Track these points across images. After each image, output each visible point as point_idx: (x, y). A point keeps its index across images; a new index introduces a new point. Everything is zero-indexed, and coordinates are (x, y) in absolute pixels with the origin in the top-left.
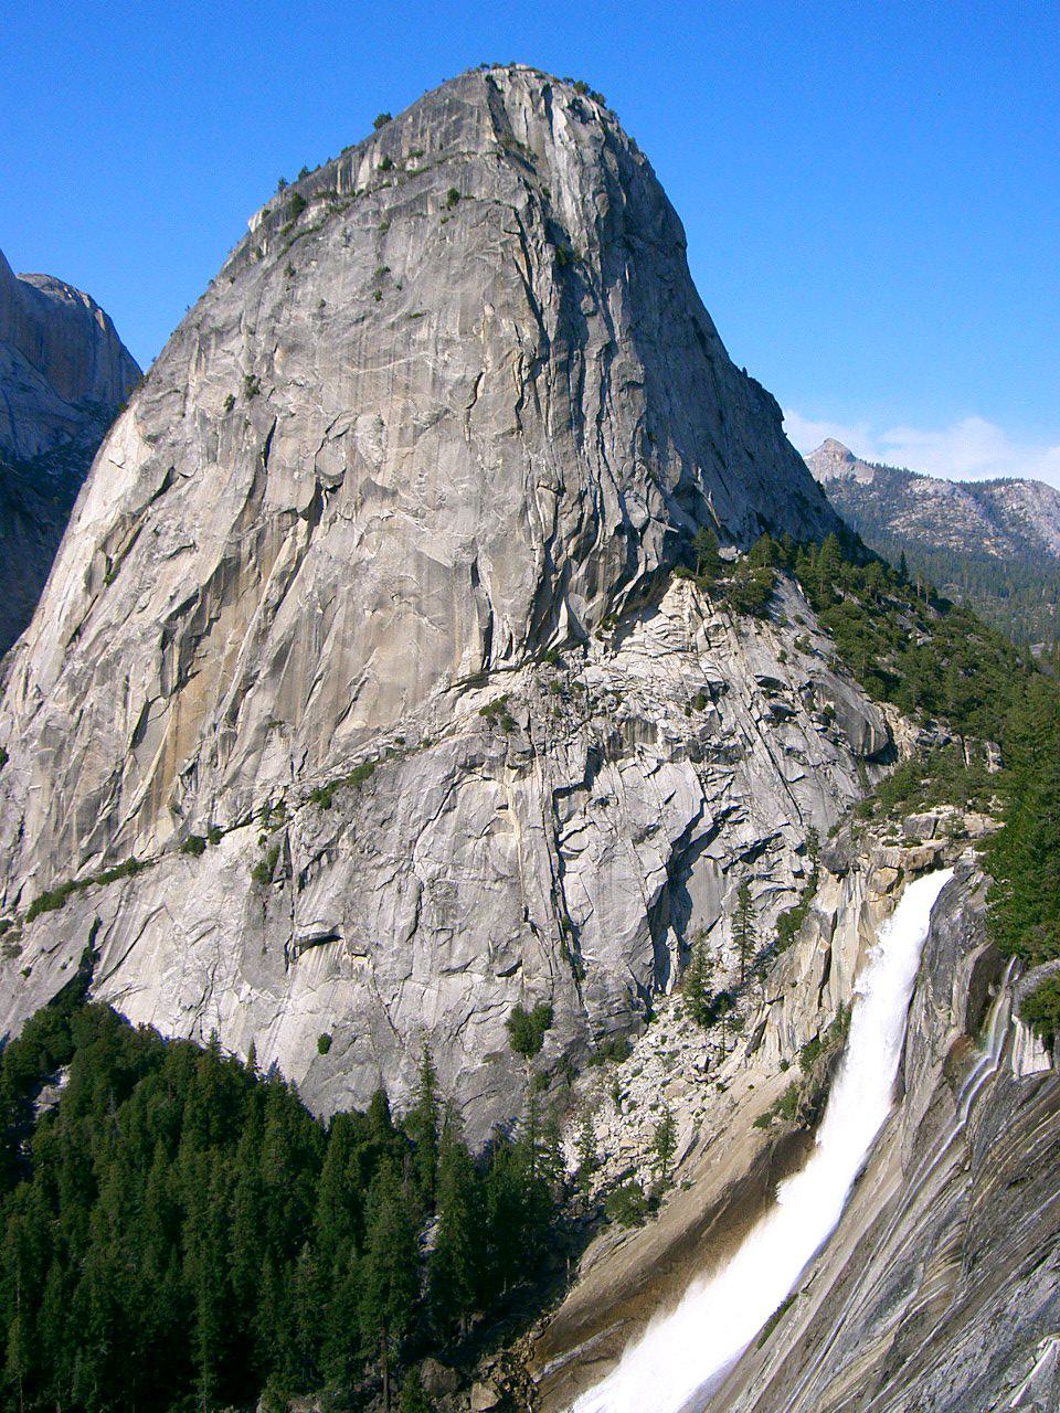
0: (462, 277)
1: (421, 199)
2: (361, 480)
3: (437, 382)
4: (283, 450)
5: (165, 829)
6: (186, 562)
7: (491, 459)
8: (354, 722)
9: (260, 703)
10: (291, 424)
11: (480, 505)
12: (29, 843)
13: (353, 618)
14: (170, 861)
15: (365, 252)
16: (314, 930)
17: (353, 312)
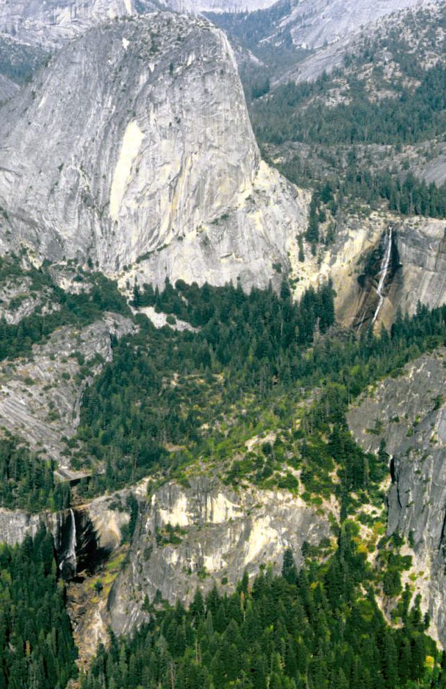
0: (229, 94)
1: (213, 72)
2: (208, 144)
3: (226, 121)
4: (189, 137)
5: (172, 235)
6: (168, 168)
7: (240, 139)
8: (217, 204)
9: (193, 202)
10: (190, 130)
11: (238, 150)
12: (133, 244)
13: (213, 179)
14: (176, 243)
15: (200, 84)
16: (225, 254)
17: (201, 101)
